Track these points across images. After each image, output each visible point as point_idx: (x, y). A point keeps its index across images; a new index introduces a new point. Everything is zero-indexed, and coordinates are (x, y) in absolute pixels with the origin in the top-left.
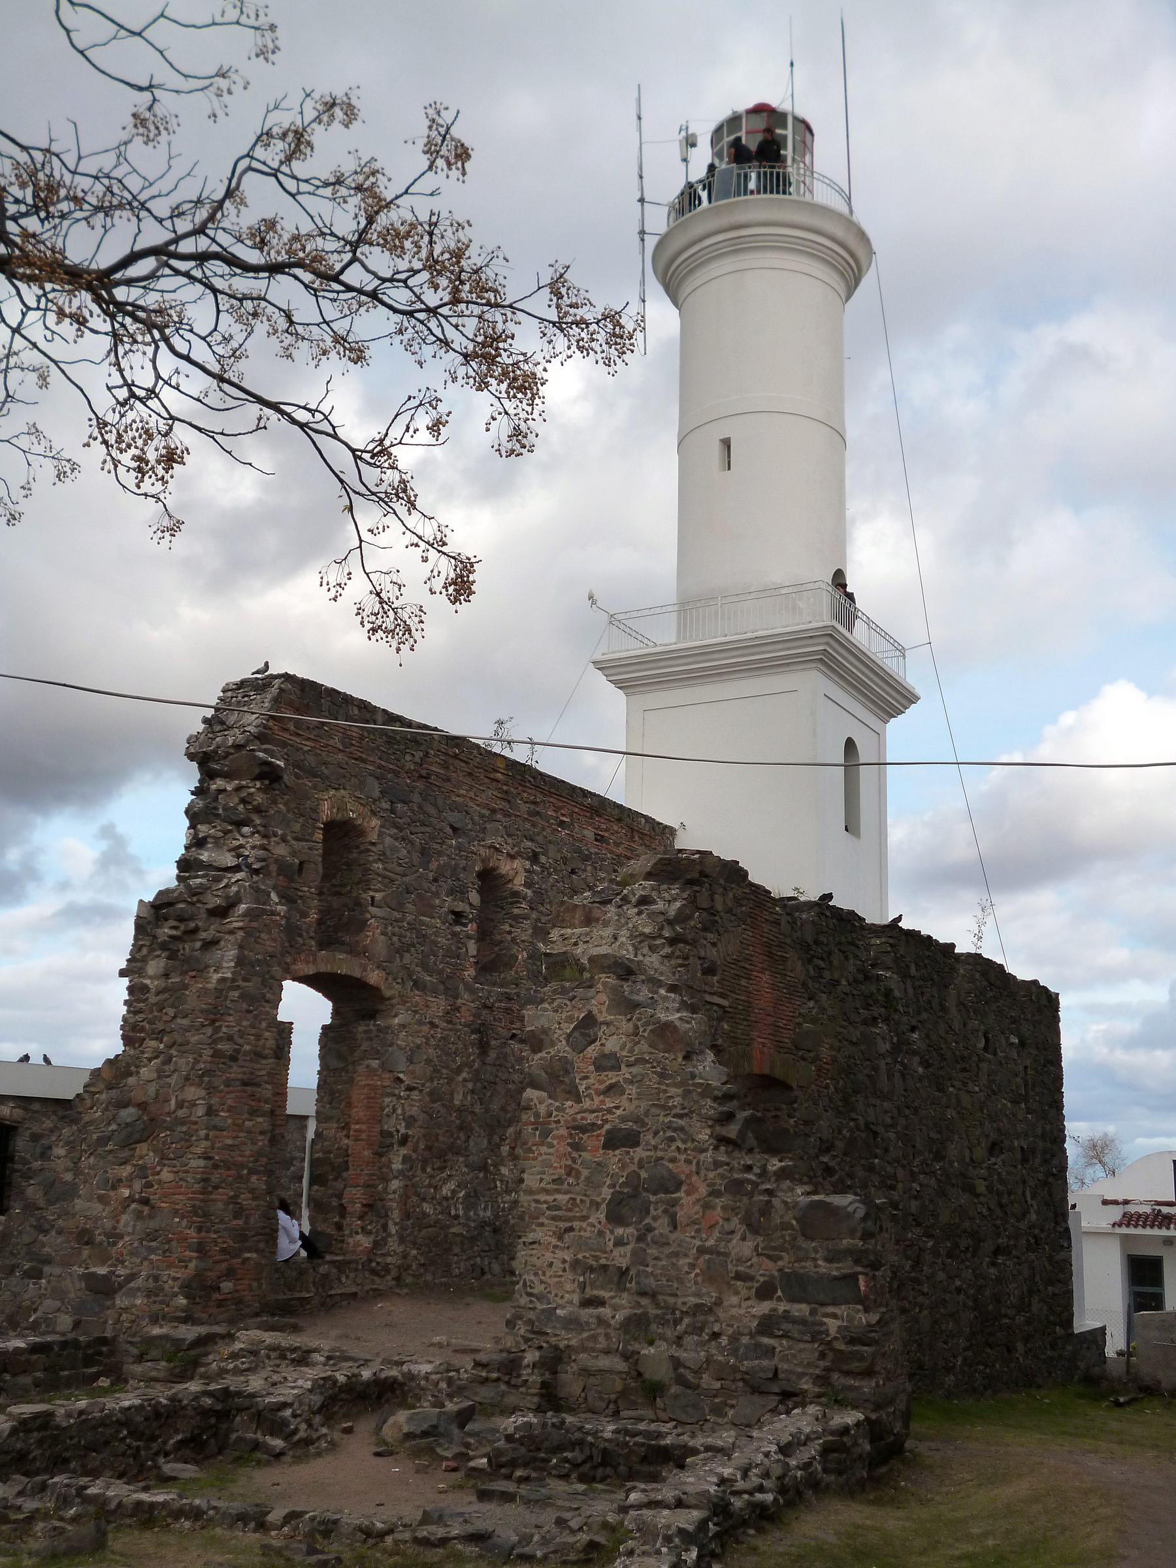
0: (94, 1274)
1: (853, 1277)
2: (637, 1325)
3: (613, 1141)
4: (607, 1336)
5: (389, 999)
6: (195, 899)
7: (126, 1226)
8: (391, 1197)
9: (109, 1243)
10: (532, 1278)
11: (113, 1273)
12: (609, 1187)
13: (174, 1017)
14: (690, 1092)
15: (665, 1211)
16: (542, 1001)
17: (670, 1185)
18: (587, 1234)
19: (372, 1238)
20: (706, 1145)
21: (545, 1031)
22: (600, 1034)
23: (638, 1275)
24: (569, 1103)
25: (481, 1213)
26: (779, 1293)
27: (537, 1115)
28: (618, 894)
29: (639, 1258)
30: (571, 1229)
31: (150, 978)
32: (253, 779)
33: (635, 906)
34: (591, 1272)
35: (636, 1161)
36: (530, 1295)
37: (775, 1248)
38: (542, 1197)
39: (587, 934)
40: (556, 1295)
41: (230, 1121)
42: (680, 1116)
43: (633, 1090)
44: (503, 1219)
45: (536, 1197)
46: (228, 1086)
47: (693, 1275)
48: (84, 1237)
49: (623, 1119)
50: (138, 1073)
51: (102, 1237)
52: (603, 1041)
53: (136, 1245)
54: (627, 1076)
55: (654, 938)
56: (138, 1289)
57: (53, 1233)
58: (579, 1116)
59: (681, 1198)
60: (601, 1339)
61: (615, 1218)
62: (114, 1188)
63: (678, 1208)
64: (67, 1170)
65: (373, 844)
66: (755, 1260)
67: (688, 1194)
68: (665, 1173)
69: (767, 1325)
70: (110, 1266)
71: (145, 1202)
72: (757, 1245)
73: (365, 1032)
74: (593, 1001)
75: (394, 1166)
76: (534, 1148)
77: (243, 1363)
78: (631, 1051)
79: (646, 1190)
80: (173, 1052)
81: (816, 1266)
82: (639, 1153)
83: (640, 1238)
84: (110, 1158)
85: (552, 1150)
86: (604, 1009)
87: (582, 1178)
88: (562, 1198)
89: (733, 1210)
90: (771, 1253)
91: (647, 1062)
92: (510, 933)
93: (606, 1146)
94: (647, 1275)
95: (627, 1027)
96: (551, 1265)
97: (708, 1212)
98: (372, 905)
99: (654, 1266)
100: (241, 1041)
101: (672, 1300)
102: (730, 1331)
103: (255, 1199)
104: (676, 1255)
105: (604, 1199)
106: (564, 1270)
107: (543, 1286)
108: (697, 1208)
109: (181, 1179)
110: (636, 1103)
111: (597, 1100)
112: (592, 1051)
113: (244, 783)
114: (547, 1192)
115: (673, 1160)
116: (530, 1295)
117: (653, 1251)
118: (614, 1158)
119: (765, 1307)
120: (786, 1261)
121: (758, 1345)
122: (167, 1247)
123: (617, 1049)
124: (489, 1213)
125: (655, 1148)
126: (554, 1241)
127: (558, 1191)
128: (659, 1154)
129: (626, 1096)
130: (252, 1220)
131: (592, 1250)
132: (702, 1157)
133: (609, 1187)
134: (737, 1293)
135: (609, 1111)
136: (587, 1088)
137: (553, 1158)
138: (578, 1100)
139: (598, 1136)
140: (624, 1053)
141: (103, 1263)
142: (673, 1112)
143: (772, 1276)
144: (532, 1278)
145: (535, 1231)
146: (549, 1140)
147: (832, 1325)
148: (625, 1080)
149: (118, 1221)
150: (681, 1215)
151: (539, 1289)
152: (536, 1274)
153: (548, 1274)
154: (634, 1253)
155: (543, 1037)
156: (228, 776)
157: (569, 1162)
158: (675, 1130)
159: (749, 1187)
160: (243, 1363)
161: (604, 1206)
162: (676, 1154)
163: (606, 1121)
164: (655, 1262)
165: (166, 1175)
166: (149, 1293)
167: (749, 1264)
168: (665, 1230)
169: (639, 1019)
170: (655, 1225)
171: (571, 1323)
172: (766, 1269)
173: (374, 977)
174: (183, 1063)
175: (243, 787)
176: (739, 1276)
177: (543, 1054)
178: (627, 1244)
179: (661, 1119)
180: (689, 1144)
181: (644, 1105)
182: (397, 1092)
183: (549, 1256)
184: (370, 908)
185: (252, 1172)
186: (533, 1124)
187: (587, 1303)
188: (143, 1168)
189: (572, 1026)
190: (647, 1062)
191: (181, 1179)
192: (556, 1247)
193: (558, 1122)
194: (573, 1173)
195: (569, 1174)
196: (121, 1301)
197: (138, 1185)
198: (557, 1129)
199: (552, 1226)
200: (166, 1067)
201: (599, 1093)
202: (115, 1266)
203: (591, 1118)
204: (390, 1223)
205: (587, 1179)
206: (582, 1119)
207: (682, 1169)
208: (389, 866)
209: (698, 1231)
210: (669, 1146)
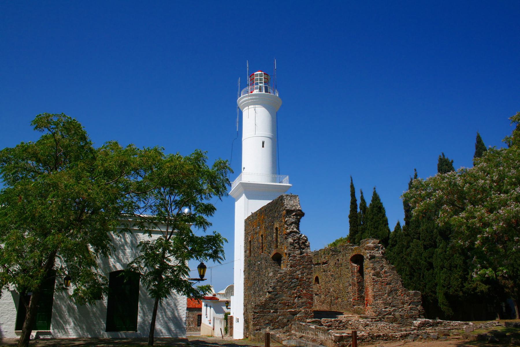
2: (394, 311)
3: (387, 284)
61: (389, 296)
69: (411, 309)
112: (383, 270)
118: (388, 287)
119: (409, 307)
171: (385, 311)
172: (409, 301)
187: (385, 308)
196: (298, 315)
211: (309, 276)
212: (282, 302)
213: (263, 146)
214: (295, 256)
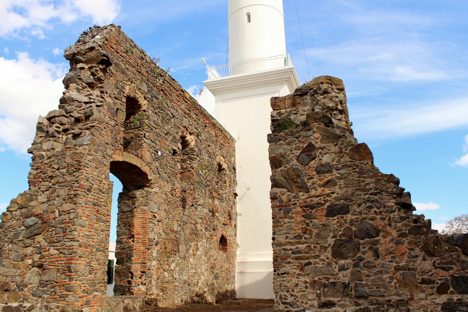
0: (10, 307)
5: (151, 180)
6: (68, 115)
7: (29, 279)
8: (153, 268)
9: (19, 290)
10: (286, 293)
11: (21, 306)
12: (332, 237)
13: (58, 169)
14: (379, 180)
15: (370, 248)
16: (279, 140)
17: (371, 233)
18: (320, 266)
19: (145, 286)
20: (394, 208)
21: (283, 157)
22: (318, 154)
23: (356, 285)
25: (184, 277)
26: (451, 289)
27: (281, 201)
28: (312, 89)
29: (356, 276)
30: (310, 263)
31: (44, 151)
32: (99, 63)
33: (321, 95)
34: (324, 287)
35: (348, 221)
36: (286, 303)
37: (445, 263)
38: (288, 247)
39: (295, 110)
40: (302, 302)
41: (87, 223)
42: (375, 194)
43: (342, 182)
44: (191, 280)
45: (284, 247)
46: (87, 204)
47: (393, 284)
49: (337, 199)
50: (37, 199)
51: (15, 286)
52: (320, 157)
53: (35, 289)
54: (338, 175)
55: (333, 110)
58: (309, 200)
59: (380, 240)
61: (338, 254)
62: (22, 260)
63: (378, 246)
65: (145, 111)
66: (434, 271)
67: (384, 237)
68: (369, 227)
70: (19, 302)
71: (40, 266)
72: (435, 262)
73: (141, 194)
74: (312, 137)
75: (153, 255)
76: (280, 220)
78: (339, 161)
79: (356, 237)
82: (349, 217)
83: (355, 265)
84: (21, 244)
85: (292, 220)
86: (318, 141)
87: (314, 234)
88: (302, 247)
89: (415, 244)
90: (445, 266)
91: (350, 166)
92: (190, 164)
93: (327, 215)
94: (363, 286)
96: (297, 285)
97: (400, 246)
98: (145, 137)
99: (366, 280)
100: (93, 182)
101: (381, 299)
103: (99, 264)
104: (381, 272)
105: (329, 245)
106: (306, 287)
107: (293, 298)
108: (391, 245)
109: (61, 253)
111: (320, 190)
112: (313, 164)
113: (94, 65)
114: (291, 244)
115: (372, 219)
116: (283, 303)
117: (365, 272)
118: (334, 221)
119: (443, 299)
120: (455, 270)
122: (52, 290)
123: (330, 161)
124: (186, 277)
125: (360, 213)
126: (298, 272)
127: (299, 243)
128: (364, 216)
129: (338, 186)
130: (98, 275)
131: (323, 274)
132: (392, 215)
133: (332, 237)
134: (423, 292)
135: (328, 195)
136: (313, 183)
137: (294, 225)
138: (307, 191)
139: (322, 209)
140: (335, 163)
141: (16, 300)
142: (370, 192)
143: (447, 280)
144: (286, 293)
145: (285, 266)
146: (290, 214)
148: (337, 178)
149: (24, 278)
150: (381, 249)
152: (288, 291)
153: (295, 290)
154: (352, 273)
155: (281, 159)
156: (86, 62)
157: (304, 226)
158: (372, 202)
159: (425, 230)
161: (330, 249)
162: (375, 215)
163: (327, 201)
164: (367, 278)
167: (430, 273)
168: (372, 259)
169: (342, 144)
170: (364, 257)
173: (145, 169)
175: (93, 67)
176: (424, 282)
177: (283, 168)
178: (347, 269)
179: (362, 197)
180: (381, 209)
181: (350, 190)
182: (154, 221)
183: (295, 280)
184: (144, 138)
185: (98, 250)
186: (279, 206)
188: (40, 248)
189: (300, 151)
190: (350, 166)
191: (61, 253)
192: (299, 275)
193: (296, 204)
194: (308, 232)
195: (305, 233)
197: (36, 257)
198: (295, 208)
199: (296, 263)
200: (53, 195)
201: (320, 186)
202: (23, 302)
203: (316, 200)
204: (153, 280)
205: (318, 235)
206: (311, 201)
207: (379, 223)
208: (151, 122)
210: (369, 211)
211: (67, 206)
213: (249, 21)
214: (42, 155)
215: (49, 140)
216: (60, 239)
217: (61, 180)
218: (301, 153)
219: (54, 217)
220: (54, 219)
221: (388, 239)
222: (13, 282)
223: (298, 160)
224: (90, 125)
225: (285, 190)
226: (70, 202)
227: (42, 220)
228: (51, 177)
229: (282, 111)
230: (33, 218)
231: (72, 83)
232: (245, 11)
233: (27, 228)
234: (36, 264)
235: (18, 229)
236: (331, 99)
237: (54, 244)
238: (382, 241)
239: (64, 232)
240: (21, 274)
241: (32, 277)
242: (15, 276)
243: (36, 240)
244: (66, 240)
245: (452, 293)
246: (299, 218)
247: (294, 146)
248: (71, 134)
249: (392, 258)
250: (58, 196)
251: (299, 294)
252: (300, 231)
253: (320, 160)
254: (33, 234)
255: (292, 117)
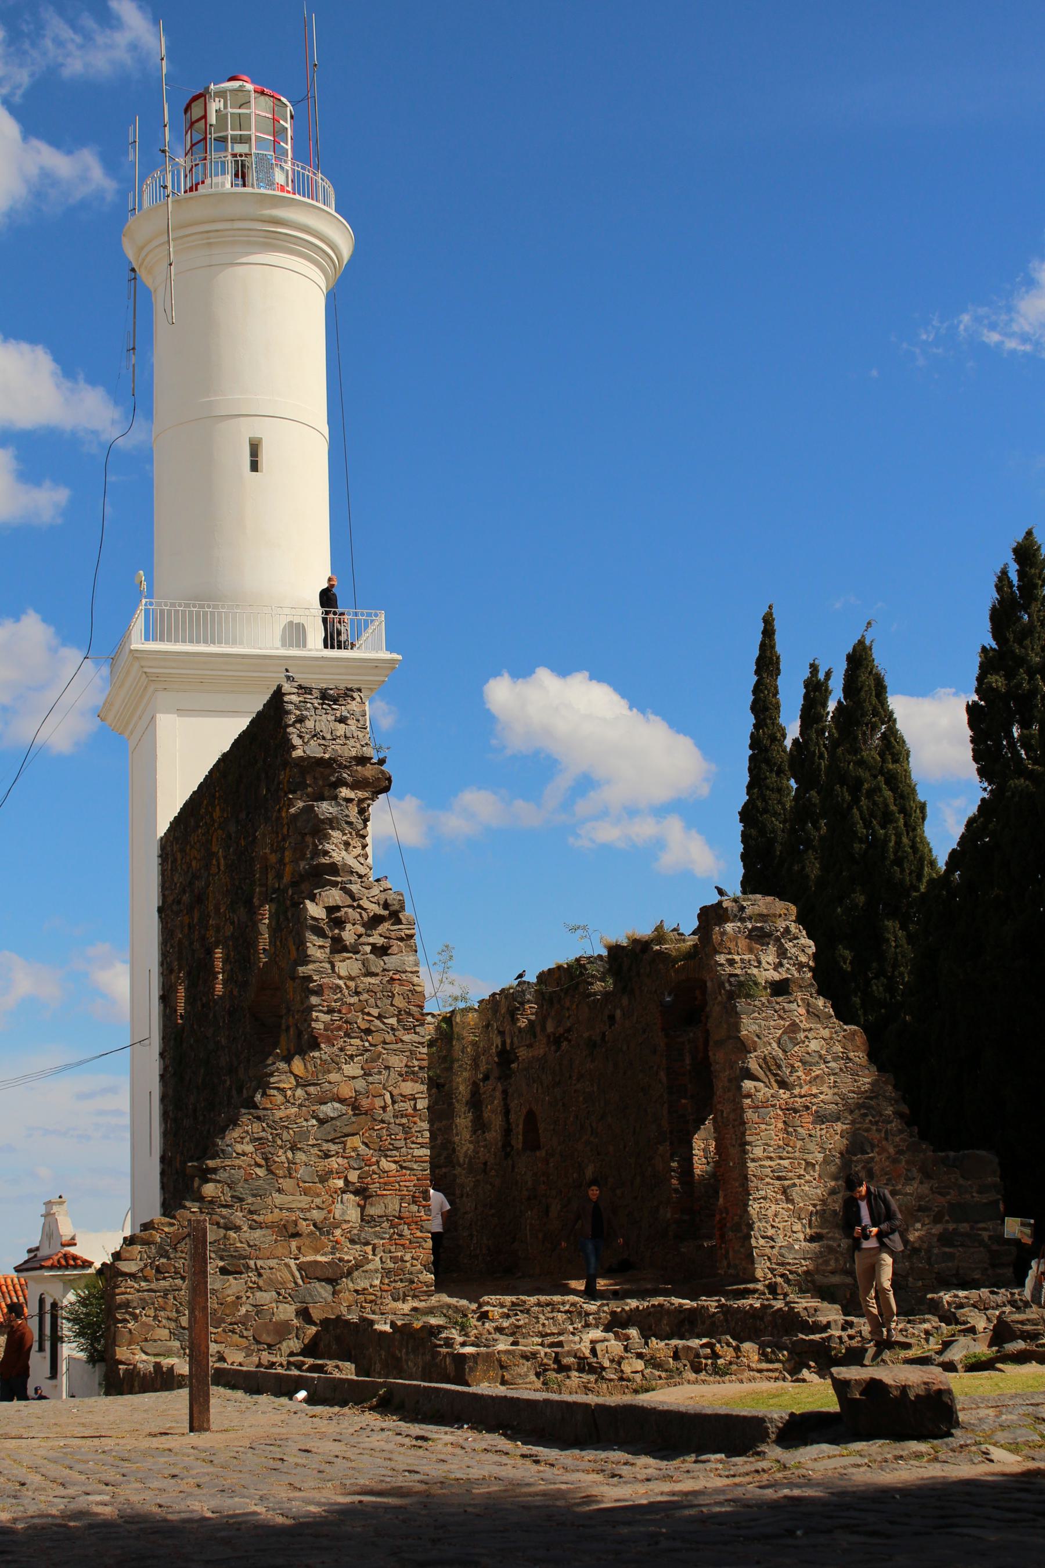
0: (316, 1262)
1: (996, 1202)
3: (821, 1118)
4: (837, 1260)
6: (355, 904)
7: (344, 1213)
11: (341, 1260)
13: (380, 1017)
15: (863, 1168)
24: (782, 1091)
26: (947, 1218)
30: (794, 1185)
31: (340, 978)
42: (871, 1098)
48: (289, 1232)
50: (340, 1069)
53: (355, 1232)
55: (803, 967)
56: (376, 1271)
57: (245, 1228)
60: (832, 1263)
62: (323, 1179)
63: (873, 1164)
64: (260, 1166)
66: (931, 1196)
69: (945, 1239)
71: (356, 1193)
77: (518, 1320)
80: (379, 1048)
81: (973, 1197)
85: (772, 1127)
95: (826, 1033)
102: (925, 1246)
110: (836, 1090)
111: (806, 1088)
114: (771, 1158)
115: (868, 1130)
116: (763, 1237)
121: (945, 1253)
127: (781, 1158)
128: (858, 1126)
132: (889, 1127)
135: (815, 1096)
147: (985, 1235)
150: (876, 1168)
151: (770, 1232)
158: (868, 1108)
160: (518, 1320)
165: (385, 1164)
166: (387, 1273)
174: (397, 1062)
191: (402, 1167)
197: (353, 1176)
207: (875, 1136)
209: (889, 1180)
212: (270, 1218)
213: (255, 467)
214: (339, 987)
215: (349, 958)
216: (398, 1144)
217: (389, 1038)
218: (783, 1033)
219: (383, 1104)
220: (384, 1108)
221: (884, 1156)
222: (305, 1220)
223: (779, 1043)
224: (408, 932)
225: (762, 1084)
226: (412, 1080)
227: (356, 1107)
228: (368, 1032)
229: (737, 958)
230: (337, 1105)
231: (333, 828)
232: (247, 430)
233: (322, 1122)
234: (351, 1188)
235: (304, 1124)
236: (803, 951)
237: (389, 1153)
238: (877, 1159)
239: (406, 1133)
240: (324, 1206)
241: (348, 1210)
242: (309, 1210)
243: (349, 1145)
244: (413, 1146)
245: (947, 1222)
246: (781, 1125)
247: (772, 1023)
248: (369, 944)
249: (888, 1180)
250: (387, 1068)
251: (780, 1225)
252: (781, 1143)
253: (807, 1046)
254: (340, 1135)
255: (755, 971)
